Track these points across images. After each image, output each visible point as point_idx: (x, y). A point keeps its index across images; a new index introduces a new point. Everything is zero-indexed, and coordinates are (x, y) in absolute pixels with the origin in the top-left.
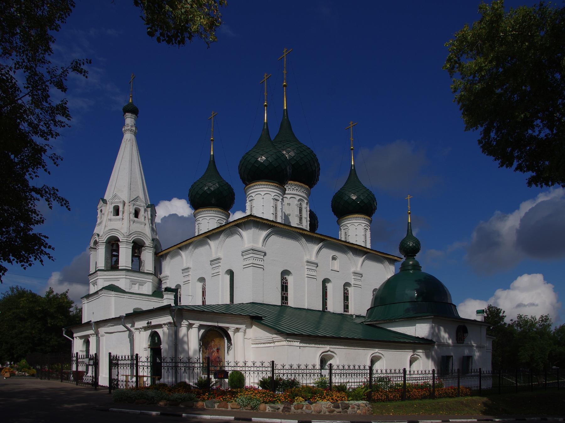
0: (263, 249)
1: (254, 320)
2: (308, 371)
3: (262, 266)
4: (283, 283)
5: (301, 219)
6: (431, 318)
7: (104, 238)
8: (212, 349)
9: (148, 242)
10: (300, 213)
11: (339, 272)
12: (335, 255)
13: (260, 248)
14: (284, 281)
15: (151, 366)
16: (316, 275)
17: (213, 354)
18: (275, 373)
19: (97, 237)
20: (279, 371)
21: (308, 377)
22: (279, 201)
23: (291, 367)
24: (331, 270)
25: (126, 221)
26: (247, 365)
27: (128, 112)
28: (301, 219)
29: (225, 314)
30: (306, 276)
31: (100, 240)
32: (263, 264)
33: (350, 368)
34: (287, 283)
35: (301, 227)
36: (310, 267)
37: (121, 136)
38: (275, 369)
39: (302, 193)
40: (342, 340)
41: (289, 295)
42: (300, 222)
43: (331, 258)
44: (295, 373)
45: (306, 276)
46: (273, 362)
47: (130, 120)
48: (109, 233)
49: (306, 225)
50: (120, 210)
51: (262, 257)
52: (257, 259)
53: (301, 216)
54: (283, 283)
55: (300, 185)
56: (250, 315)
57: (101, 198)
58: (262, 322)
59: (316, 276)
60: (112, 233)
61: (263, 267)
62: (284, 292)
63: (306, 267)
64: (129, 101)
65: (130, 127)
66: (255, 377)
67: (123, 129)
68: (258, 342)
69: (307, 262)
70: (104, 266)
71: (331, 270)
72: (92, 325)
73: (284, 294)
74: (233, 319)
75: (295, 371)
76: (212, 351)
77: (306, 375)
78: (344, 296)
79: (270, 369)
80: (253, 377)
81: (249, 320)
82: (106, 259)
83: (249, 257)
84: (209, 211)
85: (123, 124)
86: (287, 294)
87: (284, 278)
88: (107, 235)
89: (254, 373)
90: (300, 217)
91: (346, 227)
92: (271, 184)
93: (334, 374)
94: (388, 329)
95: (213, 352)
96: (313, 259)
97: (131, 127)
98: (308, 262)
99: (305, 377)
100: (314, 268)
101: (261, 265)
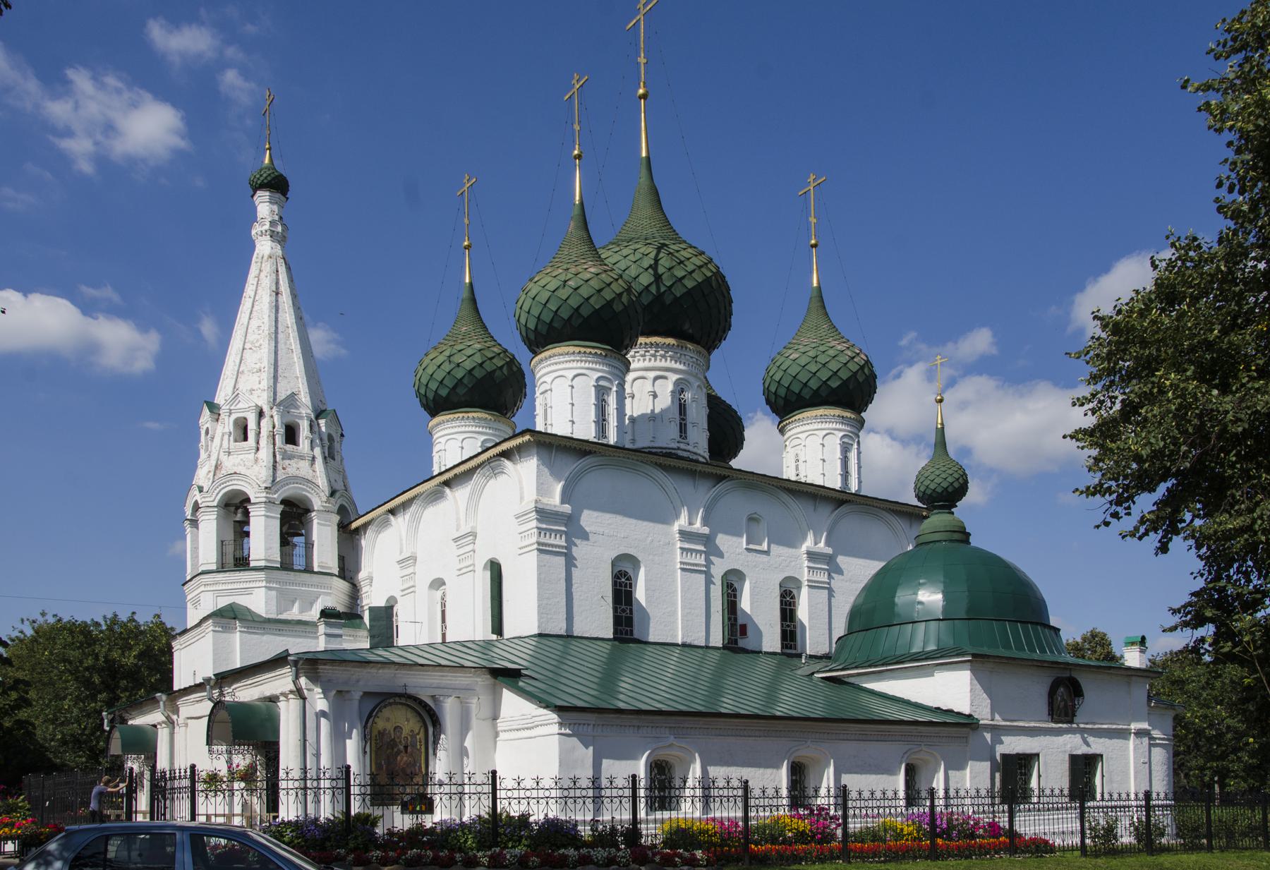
1: (500, 678)
2: (578, 793)
4: (621, 585)
5: (683, 429)
6: (968, 661)
7: (214, 496)
8: (396, 745)
9: (318, 500)
10: (680, 414)
13: (555, 506)
14: (623, 580)
15: (267, 789)
17: (399, 758)
18: (498, 797)
19: (197, 492)
20: (509, 794)
21: (578, 807)
23: (538, 783)
25: (265, 454)
26: (541, 785)
27: (262, 186)
28: (683, 429)
29: (422, 665)
31: (203, 500)
33: (716, 784)
34: (631, 587)
35: (682, 446)
36: (687, 546)
37: (249, 247)
38: (498, 788)
39: (663, 360)
40: (732, 720)
41: (634, 612)
42: (681, 436)
43: (745, 519)
44: (566, 797)
46: (494, 773)
47: (265, 206)
48: (225, 483)
49: (699, 441)
50: (249, 428)
53: (683, 420)
54: (621, 585)
56: (485, 667)
57: (206, 402)
58: (521, 684)
60: (231, 483)
62: (623, 607)
64: (263, 162)
65: (268, 224)
66: (453, 806)
67: (253, 232)
68: (506, 728)
70: (215, 561)
72: (158, 702)
73: (624, 611)
74: (447, 676)
75: (547, 794)
76: (396, 750)
77: (575, 801)
78: (783, 612)
79: (487, 789)
80: (448, 806)
81: (489, 676)
82: (222, 544)
84: (452, 420)
85: (252, 217)
86: (631, 610)
87: (625, 576)
88: (220, 488)
89: (451, 798)
90: (681, 424)
91: (796, 442)
93: (753, 809)
94: (864, 685)
95: (399, 752)
97: (271, 226)
99: (572, 806)
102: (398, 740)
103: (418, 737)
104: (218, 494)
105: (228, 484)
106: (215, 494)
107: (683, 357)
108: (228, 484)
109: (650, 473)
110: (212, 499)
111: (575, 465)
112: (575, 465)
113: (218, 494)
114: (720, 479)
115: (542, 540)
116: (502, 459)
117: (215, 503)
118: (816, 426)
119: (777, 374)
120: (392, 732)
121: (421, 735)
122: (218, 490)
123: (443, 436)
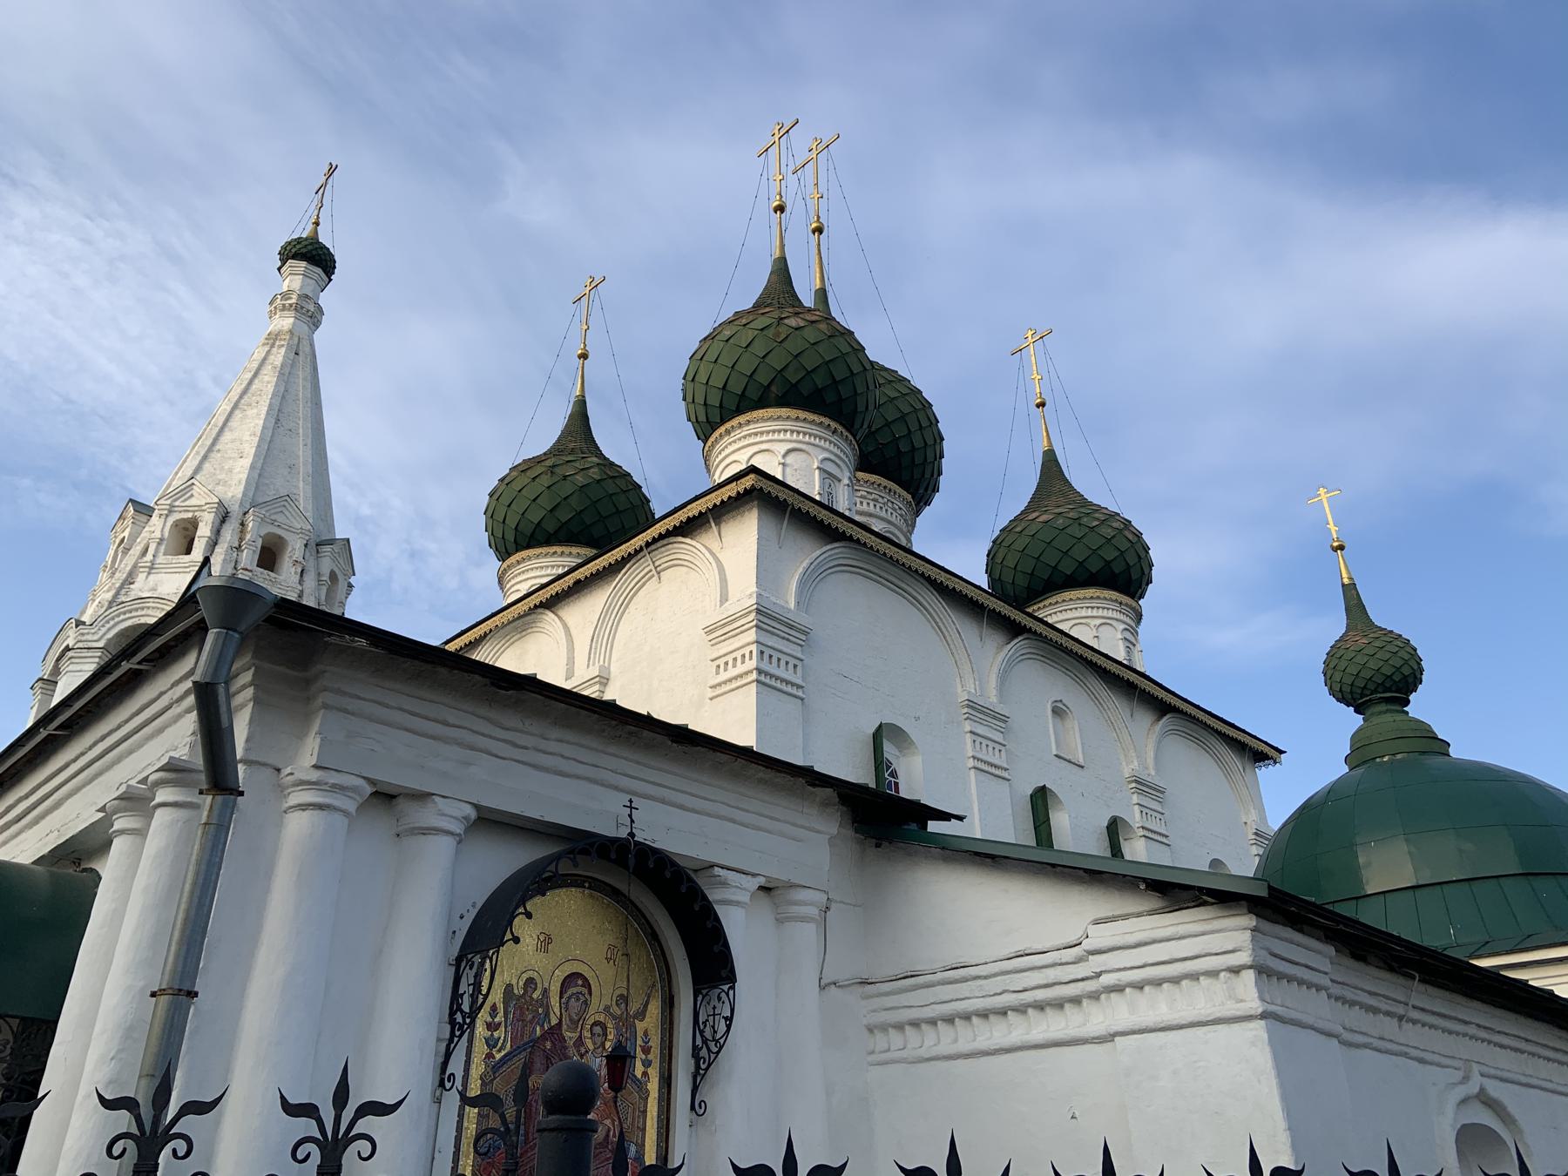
0: (802, 619)
3: (799, 687)
11: (1082, 767)
12: (1061, 701)
16: (1005, 766)
22: (840, 481)
24: (1056, 756)
30: (971, 763)
32: (799, 682)
34: (896, 784)
36: (980, 730)
45: (971, 763)
51: (797, 652)
52: (776, 655)
55: (885, 487)
59: (1006, 769)
61: (800, 693)
63: (968, 726)
69: (968, 706)
71: (1056, 756)
83: (740, 644)
92: (811, 417)
96: (991, 698)
98: (971, 704)
100: (998, 737)
101: (793, 684)
102: (570, 1036)
103: (640, 1026)
104: (109, 629)
105: (134, 614)
106: (104, 630)
107: (890, 504)
108: (134, 614)
109: (923, 594)
110: (96, 638)
111: (825, 549)
112: (818, 552)
113: (109, 629)
114: (1014, 630)
115: (765, 666)
116: (680, 539)
117: (101, 644)
118: (1084, 613)
119: (1009, 557)
120: (555, 989)
121: (651, 1022)
122: (112, 623)
123: (528, 579)
